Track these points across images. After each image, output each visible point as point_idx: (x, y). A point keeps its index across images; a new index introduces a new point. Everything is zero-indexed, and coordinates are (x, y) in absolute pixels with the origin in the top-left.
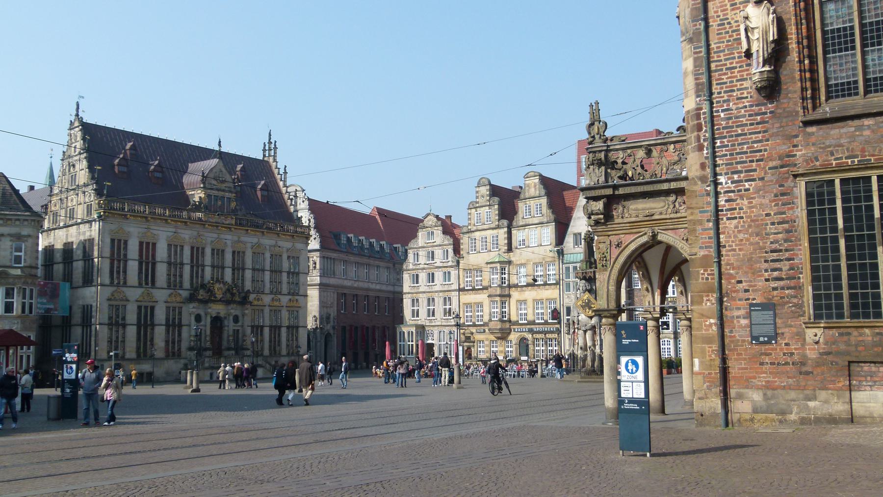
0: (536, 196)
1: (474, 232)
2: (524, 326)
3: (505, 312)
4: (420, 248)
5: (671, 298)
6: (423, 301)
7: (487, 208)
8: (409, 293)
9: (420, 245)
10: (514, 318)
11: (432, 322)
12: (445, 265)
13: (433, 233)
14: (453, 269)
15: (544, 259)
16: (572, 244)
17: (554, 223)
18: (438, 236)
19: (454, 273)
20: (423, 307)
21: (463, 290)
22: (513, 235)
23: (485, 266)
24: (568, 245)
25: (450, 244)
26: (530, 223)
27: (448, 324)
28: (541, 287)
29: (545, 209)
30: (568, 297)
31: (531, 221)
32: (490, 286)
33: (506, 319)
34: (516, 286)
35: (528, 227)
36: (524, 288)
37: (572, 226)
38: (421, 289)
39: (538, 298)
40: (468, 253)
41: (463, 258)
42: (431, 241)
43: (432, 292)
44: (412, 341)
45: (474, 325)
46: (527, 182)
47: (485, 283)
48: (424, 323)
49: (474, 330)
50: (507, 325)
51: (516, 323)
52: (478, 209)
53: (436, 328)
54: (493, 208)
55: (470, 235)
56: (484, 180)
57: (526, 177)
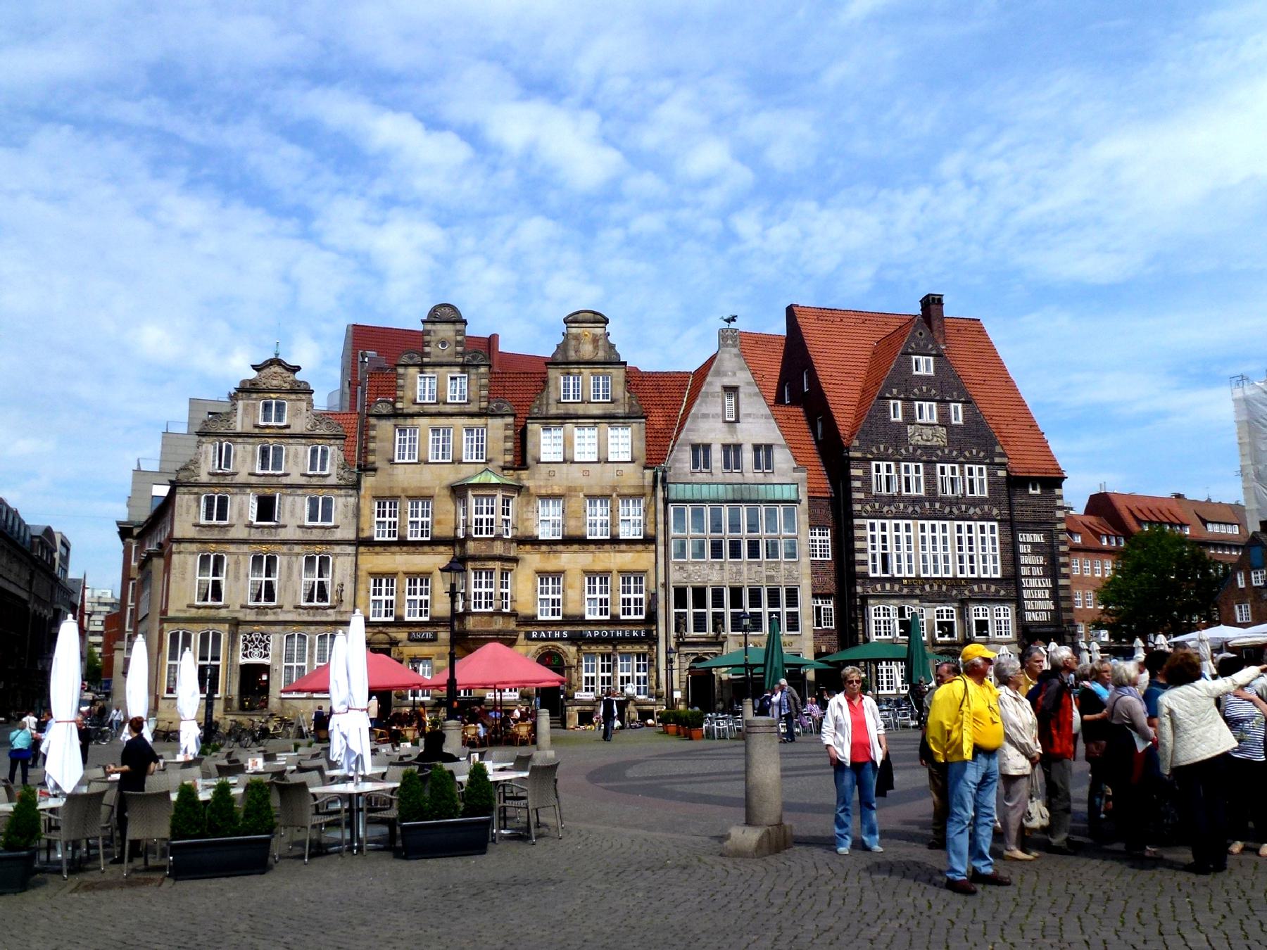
0: (596, 359)
1: (412, 415)
2: (554, 628)
3: (507, 594)
4: (239, 435)
5: (905, 578)
6: (237, 563)
7: (458, 369)
8: (192, 541)
9: (239, 429)
10: (524, 610)
11: (267, 614)
12: (314, 481)
13: (280, 407)
14: (342, 492)
15: (614, 488)
16: (688, 465)
17: (644, 420)
18: (296, 413)
19: (341, 504)
20: (237, 578)
21: (369, 543)
22: (529, 434)
23: (446, 492)
24: (677, 465)
25: (336, 437)
26: (581, 412)
27: (318, 619)
28: (607, 547)
29: (619, 391)
30: (681, 568)
31: (581, 409)
32: (468, 537)
33: (508, 610)
34: (534, 542)
35: (574, 421)
36: (560, 548)
37: (688, 430)
38: (233, 534)
39: (598, 567)
40: (391, 462)
41: (375, 470)
42: (273, 423)
43: (274, 542)
44: (216, 658)
45: (399, 623)
46: (574, 331)
47: (445, 531)
48: (241, 616)
49: (401, 635)
50: (512, 625)
51: (530, 621)
52: (428, 370)
53: (278, 628)
54: (473, 371)
55: (401, 421)
56: (447, 310)
57: (571, 320)
